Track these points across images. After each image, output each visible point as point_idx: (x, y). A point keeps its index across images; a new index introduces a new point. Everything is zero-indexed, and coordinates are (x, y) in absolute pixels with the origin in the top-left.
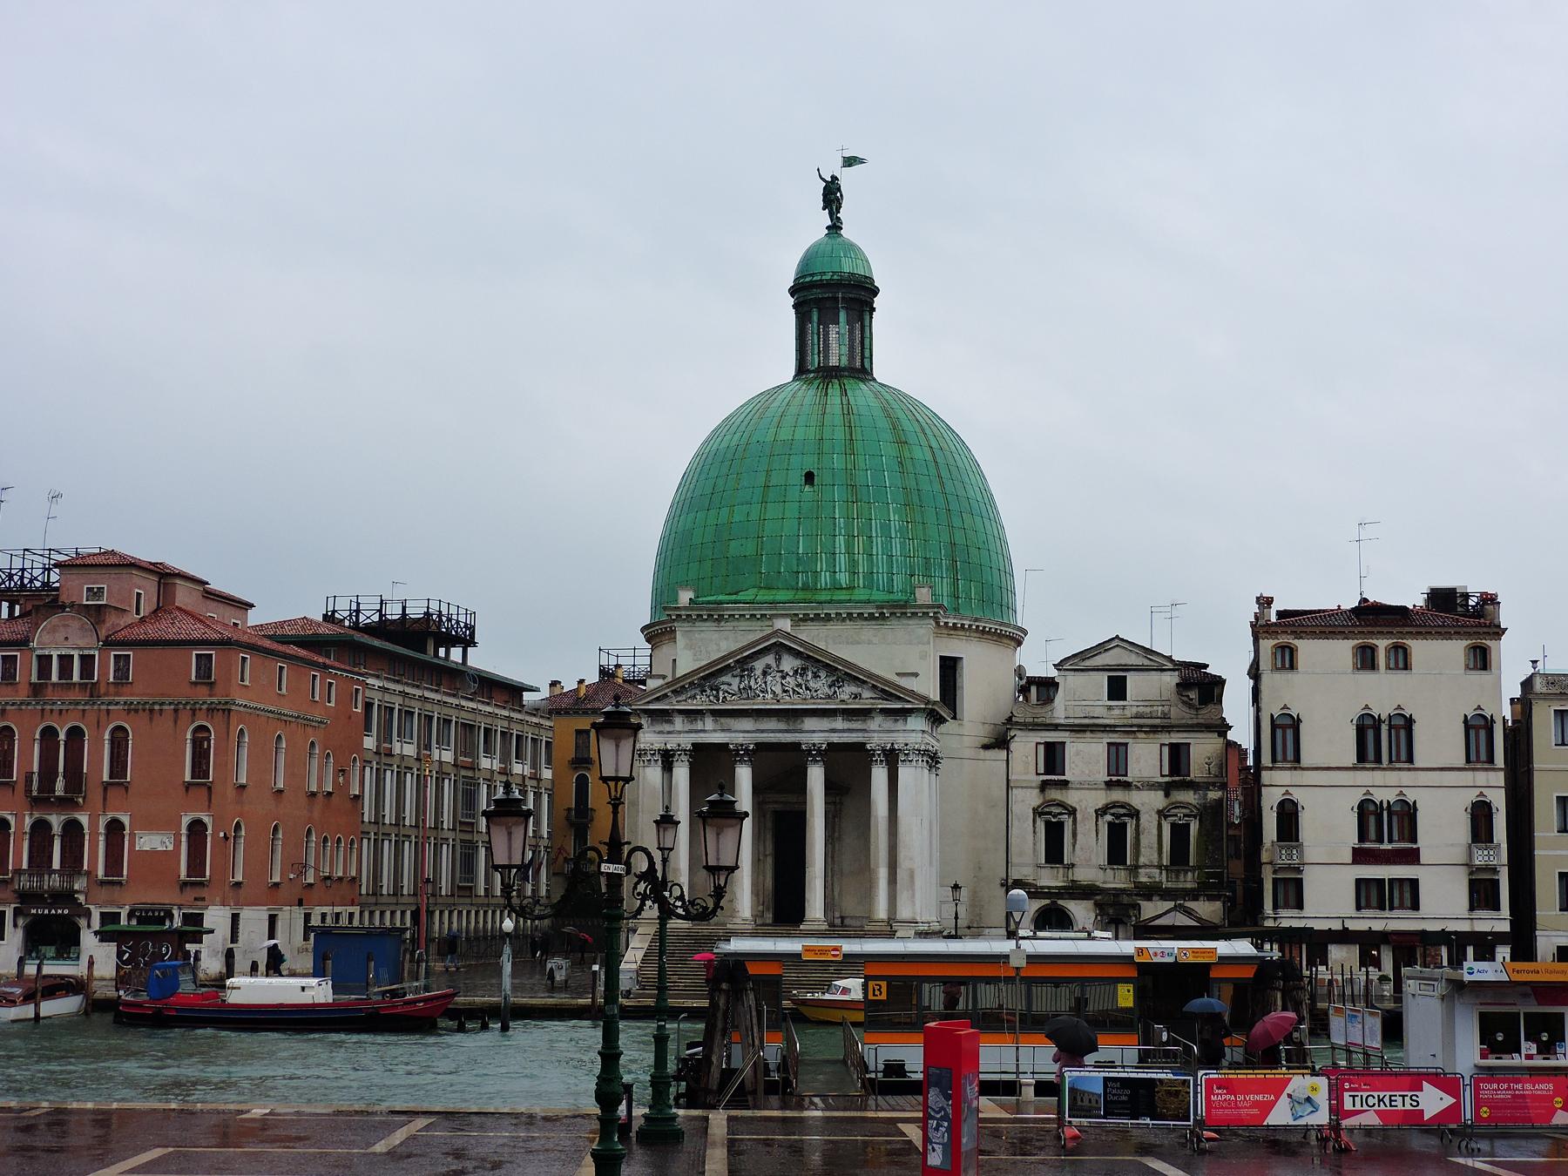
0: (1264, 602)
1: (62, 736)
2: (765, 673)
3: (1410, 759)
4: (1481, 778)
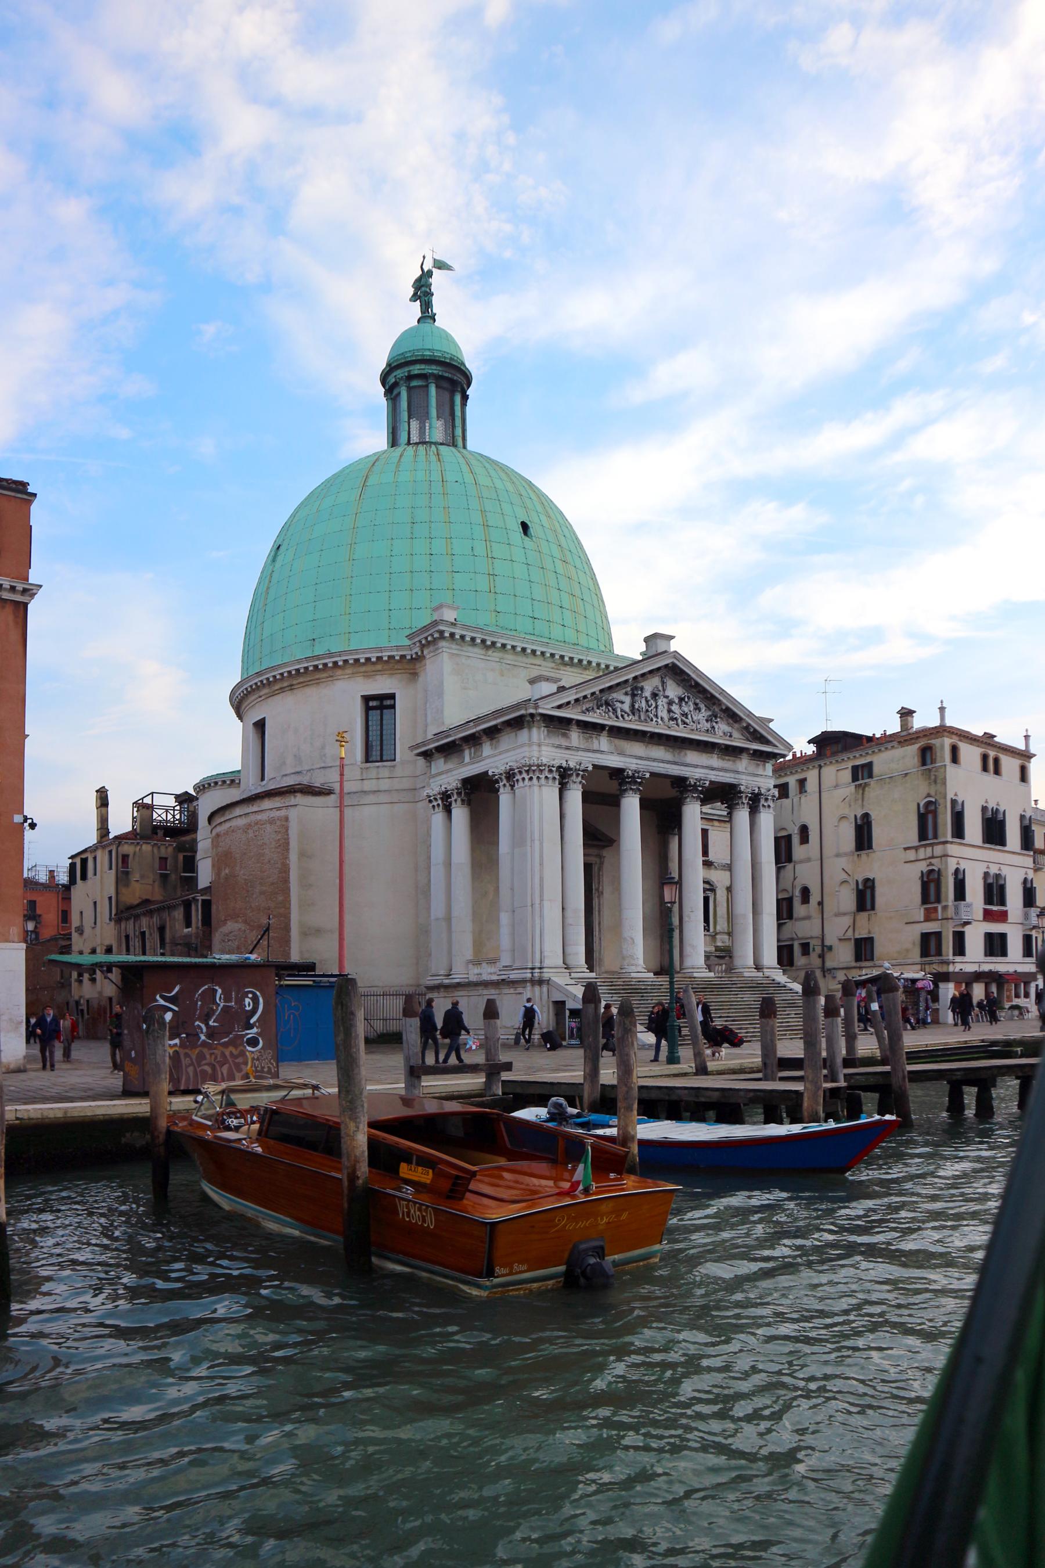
2: (655, 695)
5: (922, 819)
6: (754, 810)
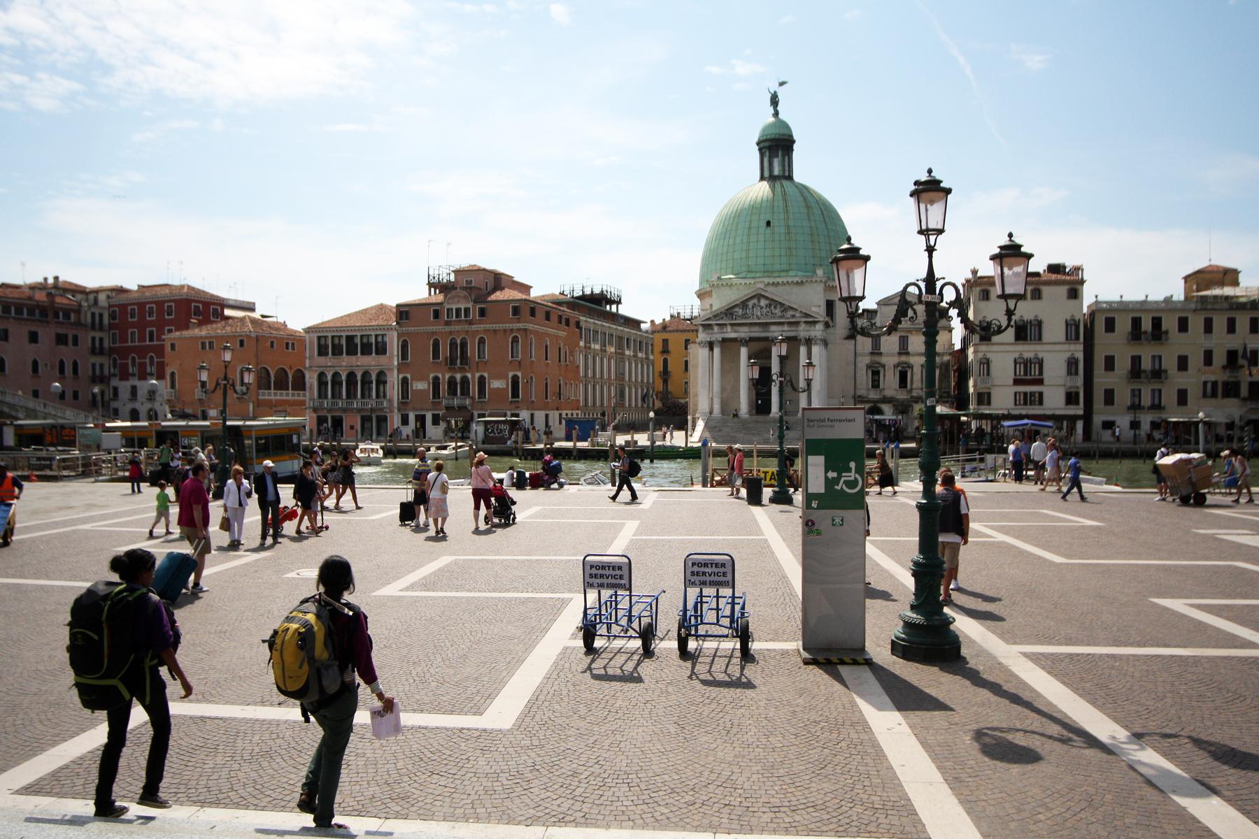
0: (975, 272)
3: (1040, 339)
4: (1072, 347)
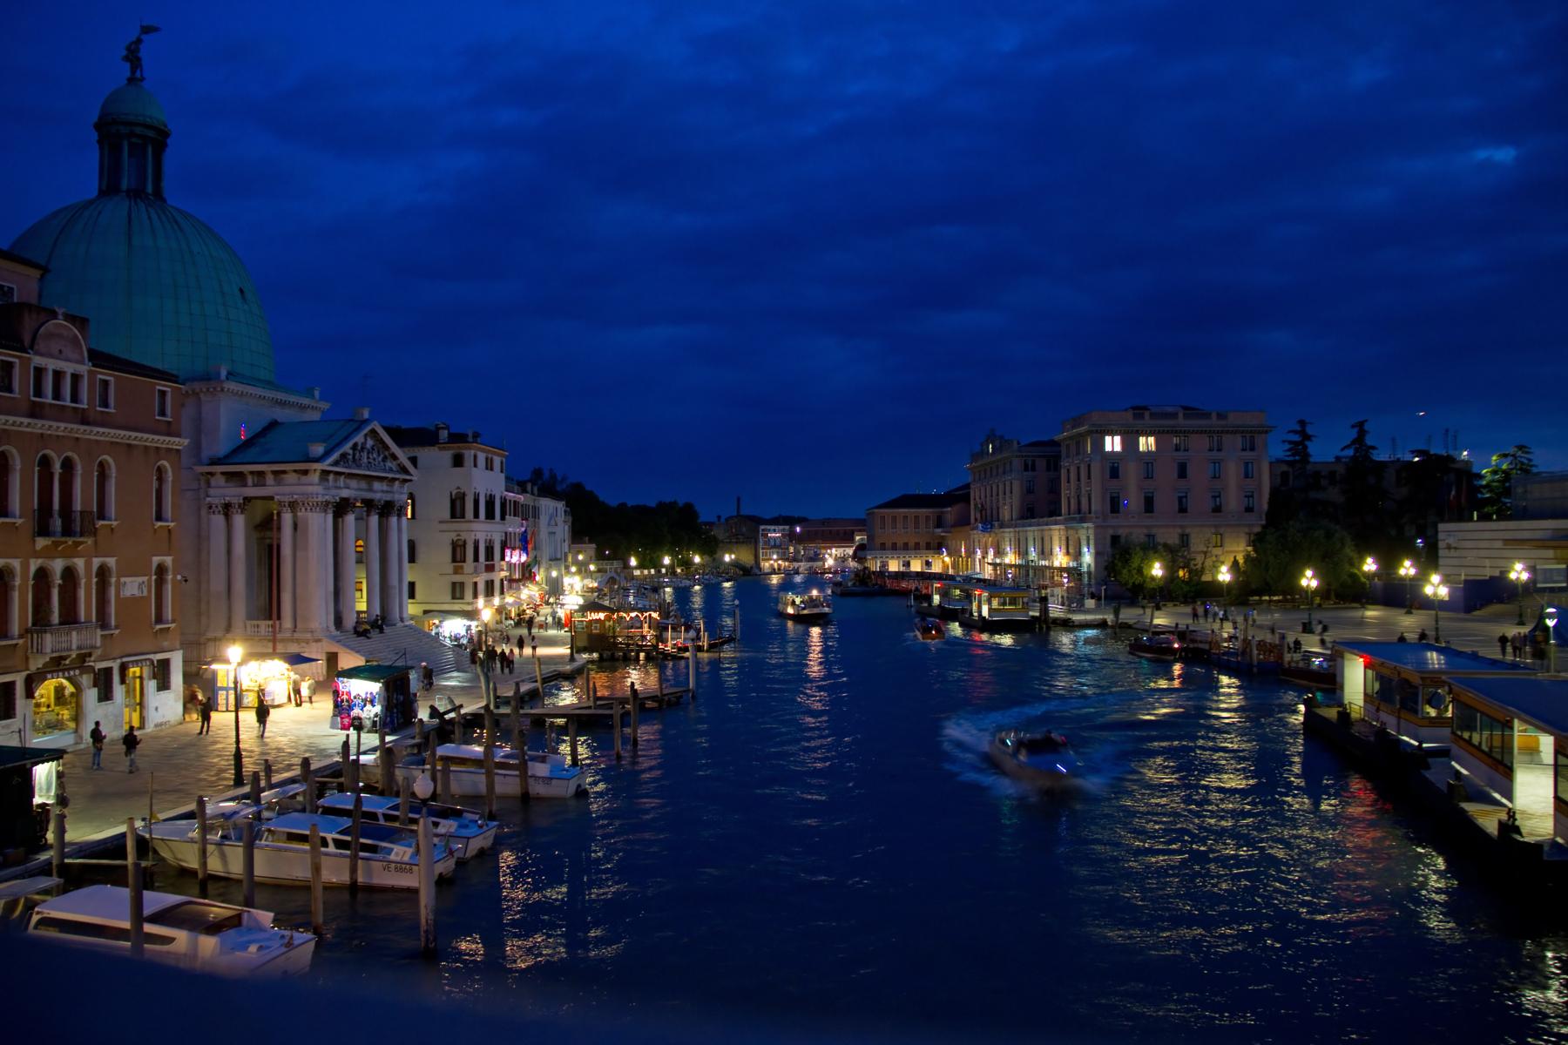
1: (57, 468)
5: (453, 502)
6: (399, 516)
